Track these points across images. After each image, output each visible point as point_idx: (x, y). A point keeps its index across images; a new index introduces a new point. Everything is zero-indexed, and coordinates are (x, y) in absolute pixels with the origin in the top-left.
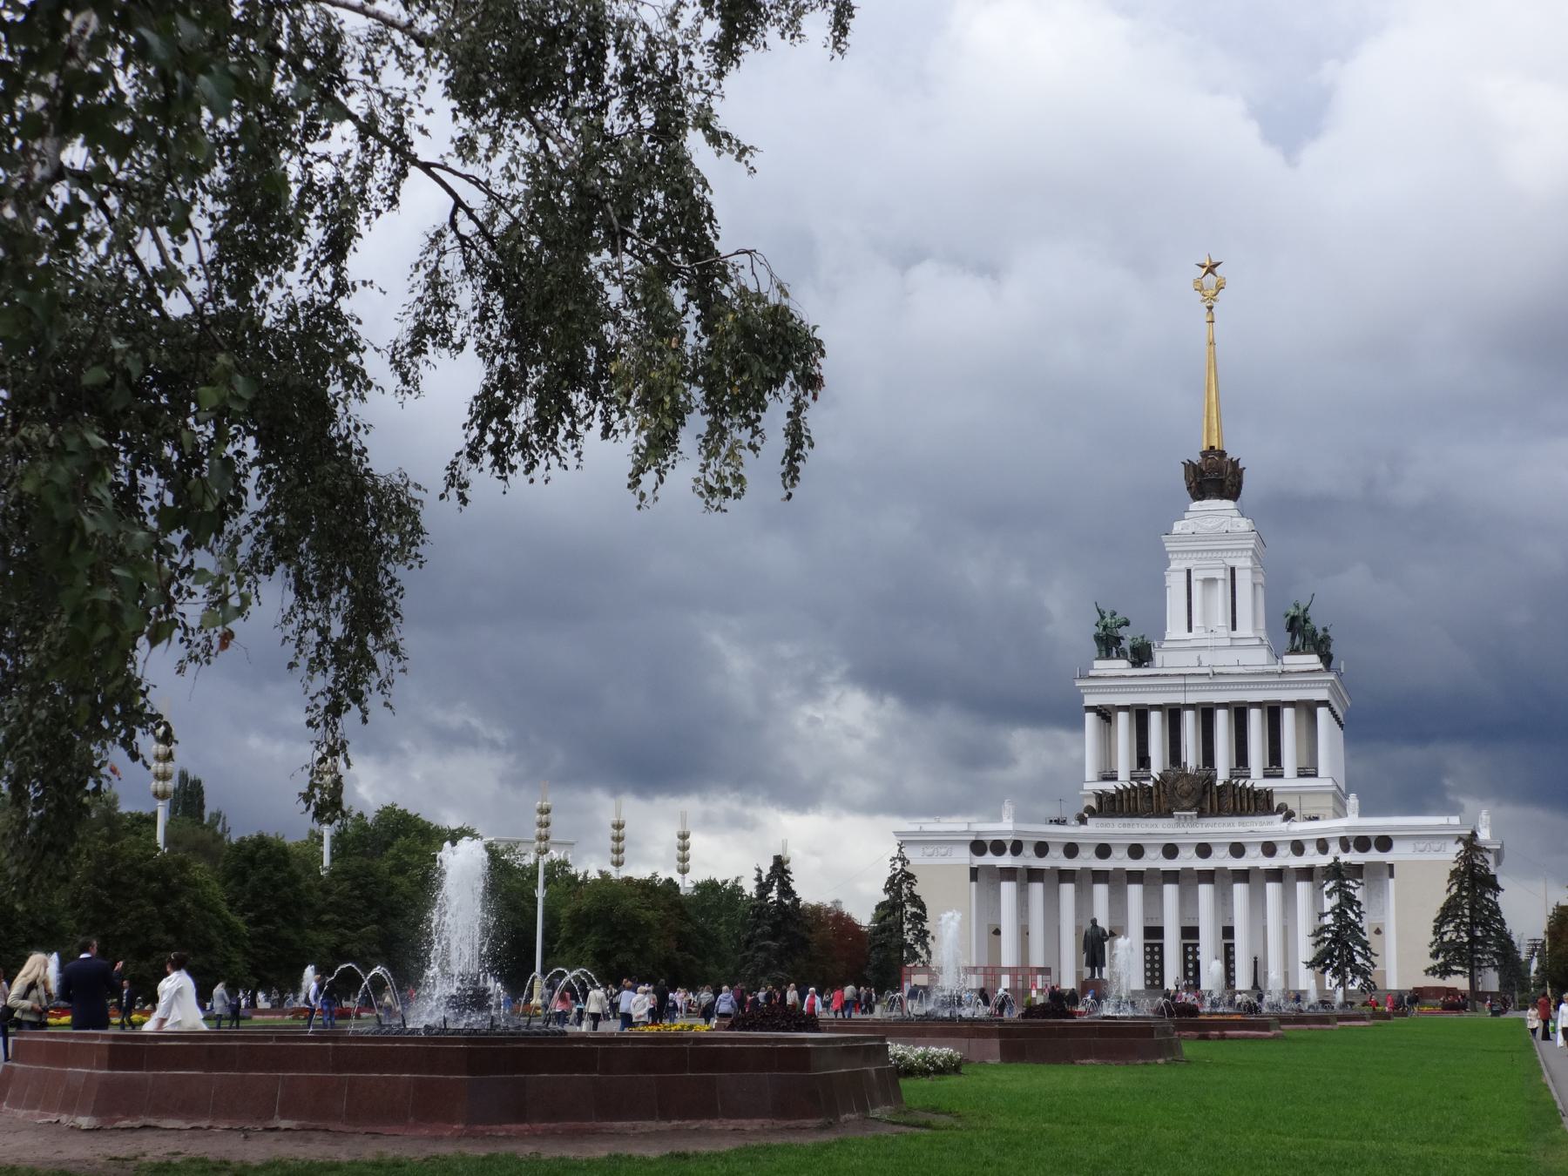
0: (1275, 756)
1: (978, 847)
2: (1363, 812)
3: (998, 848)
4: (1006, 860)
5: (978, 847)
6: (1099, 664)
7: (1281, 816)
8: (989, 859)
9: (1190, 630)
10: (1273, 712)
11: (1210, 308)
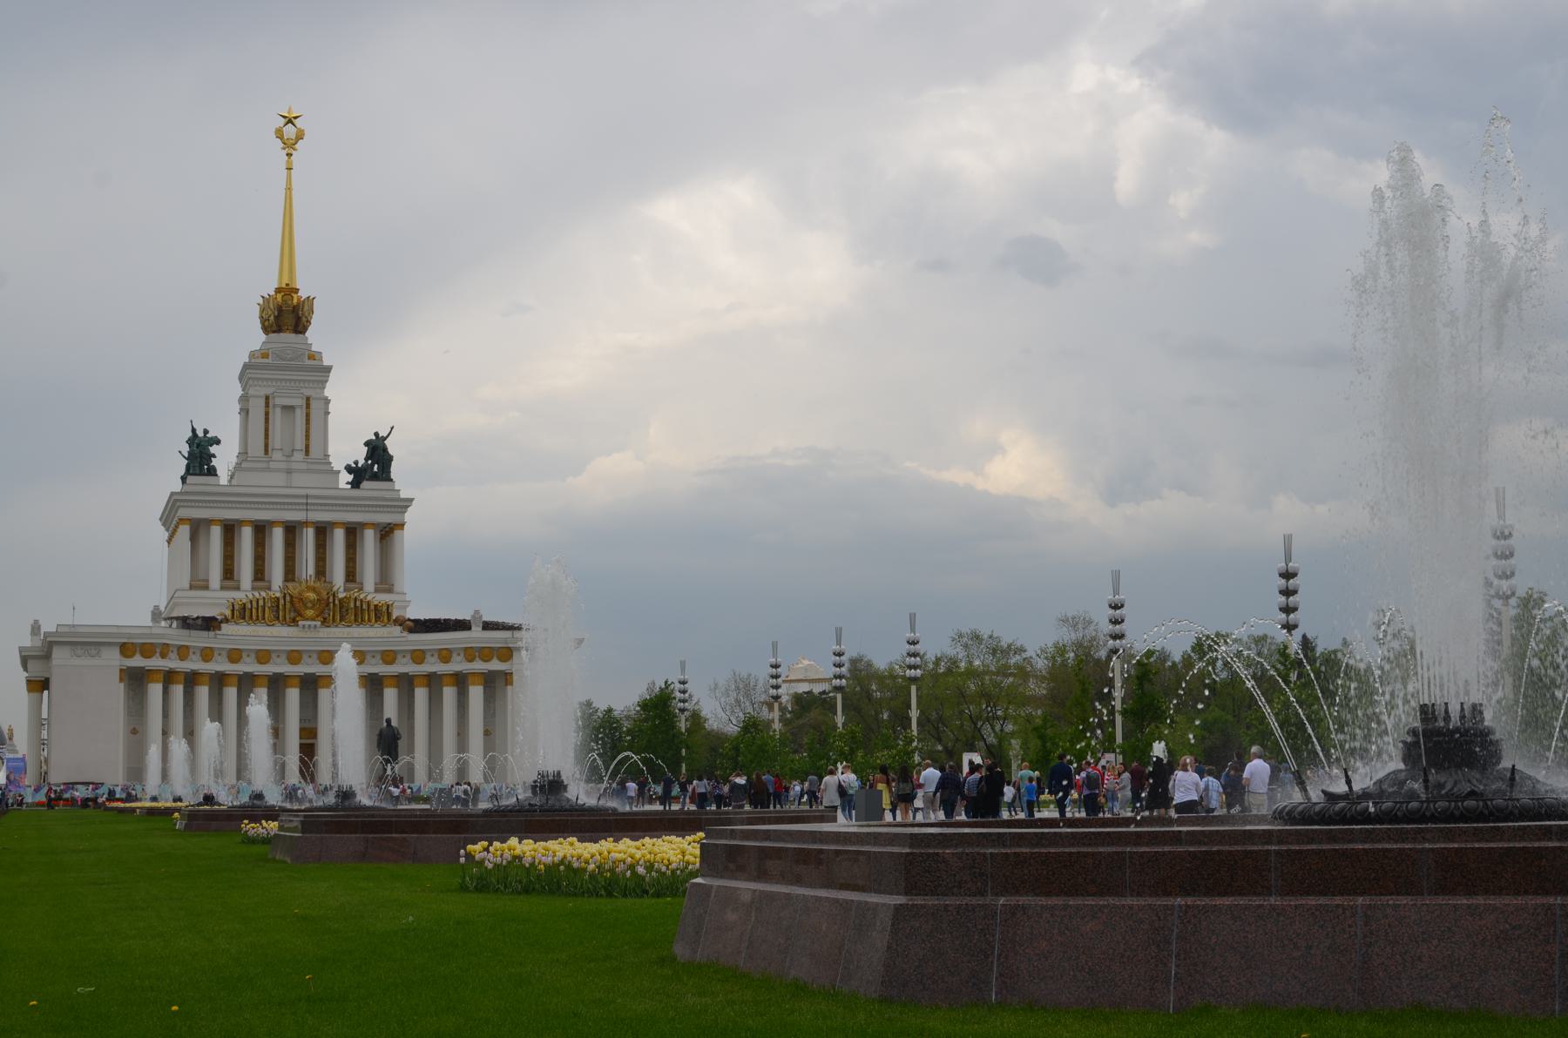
0: (351, 575)
1: (126, 649)
3: (147, 650)
4: (156, 663)
5: (126, 649)
10: (353, 533)
11: (290, 155)
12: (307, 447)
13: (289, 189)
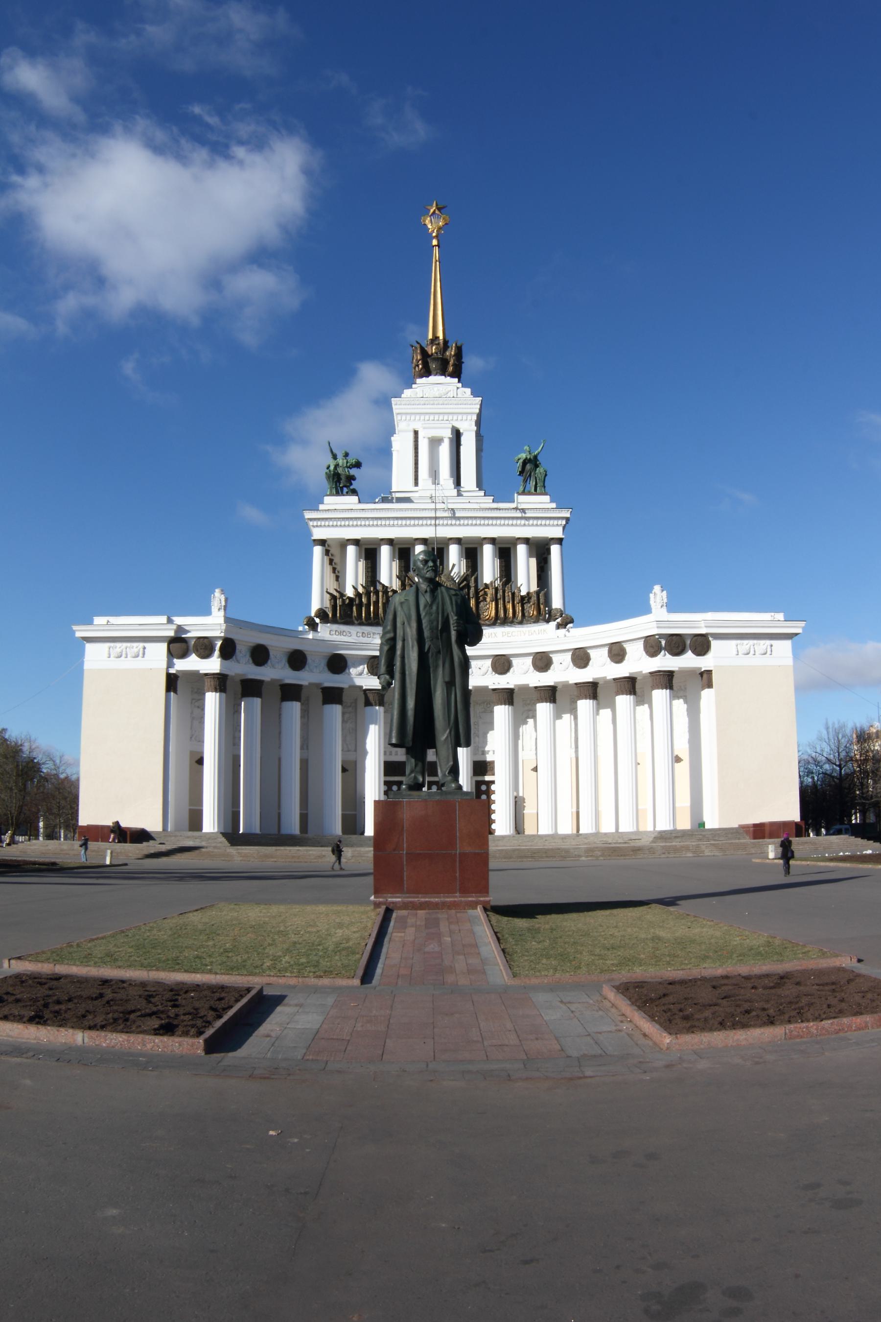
2: (672, 606)
3: (204, 647)
4: (213, 665)
6: (327, 499)
7: (553, 624)
8: (192, 663)
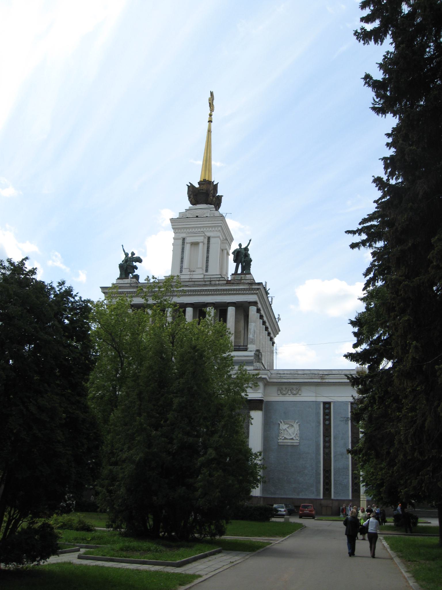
9: (181, 271)
12: (207, 267)
13: (209, 131)
